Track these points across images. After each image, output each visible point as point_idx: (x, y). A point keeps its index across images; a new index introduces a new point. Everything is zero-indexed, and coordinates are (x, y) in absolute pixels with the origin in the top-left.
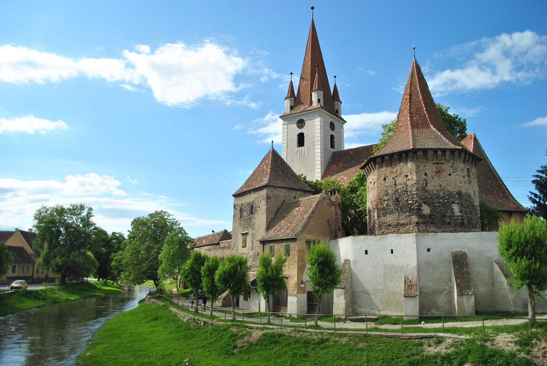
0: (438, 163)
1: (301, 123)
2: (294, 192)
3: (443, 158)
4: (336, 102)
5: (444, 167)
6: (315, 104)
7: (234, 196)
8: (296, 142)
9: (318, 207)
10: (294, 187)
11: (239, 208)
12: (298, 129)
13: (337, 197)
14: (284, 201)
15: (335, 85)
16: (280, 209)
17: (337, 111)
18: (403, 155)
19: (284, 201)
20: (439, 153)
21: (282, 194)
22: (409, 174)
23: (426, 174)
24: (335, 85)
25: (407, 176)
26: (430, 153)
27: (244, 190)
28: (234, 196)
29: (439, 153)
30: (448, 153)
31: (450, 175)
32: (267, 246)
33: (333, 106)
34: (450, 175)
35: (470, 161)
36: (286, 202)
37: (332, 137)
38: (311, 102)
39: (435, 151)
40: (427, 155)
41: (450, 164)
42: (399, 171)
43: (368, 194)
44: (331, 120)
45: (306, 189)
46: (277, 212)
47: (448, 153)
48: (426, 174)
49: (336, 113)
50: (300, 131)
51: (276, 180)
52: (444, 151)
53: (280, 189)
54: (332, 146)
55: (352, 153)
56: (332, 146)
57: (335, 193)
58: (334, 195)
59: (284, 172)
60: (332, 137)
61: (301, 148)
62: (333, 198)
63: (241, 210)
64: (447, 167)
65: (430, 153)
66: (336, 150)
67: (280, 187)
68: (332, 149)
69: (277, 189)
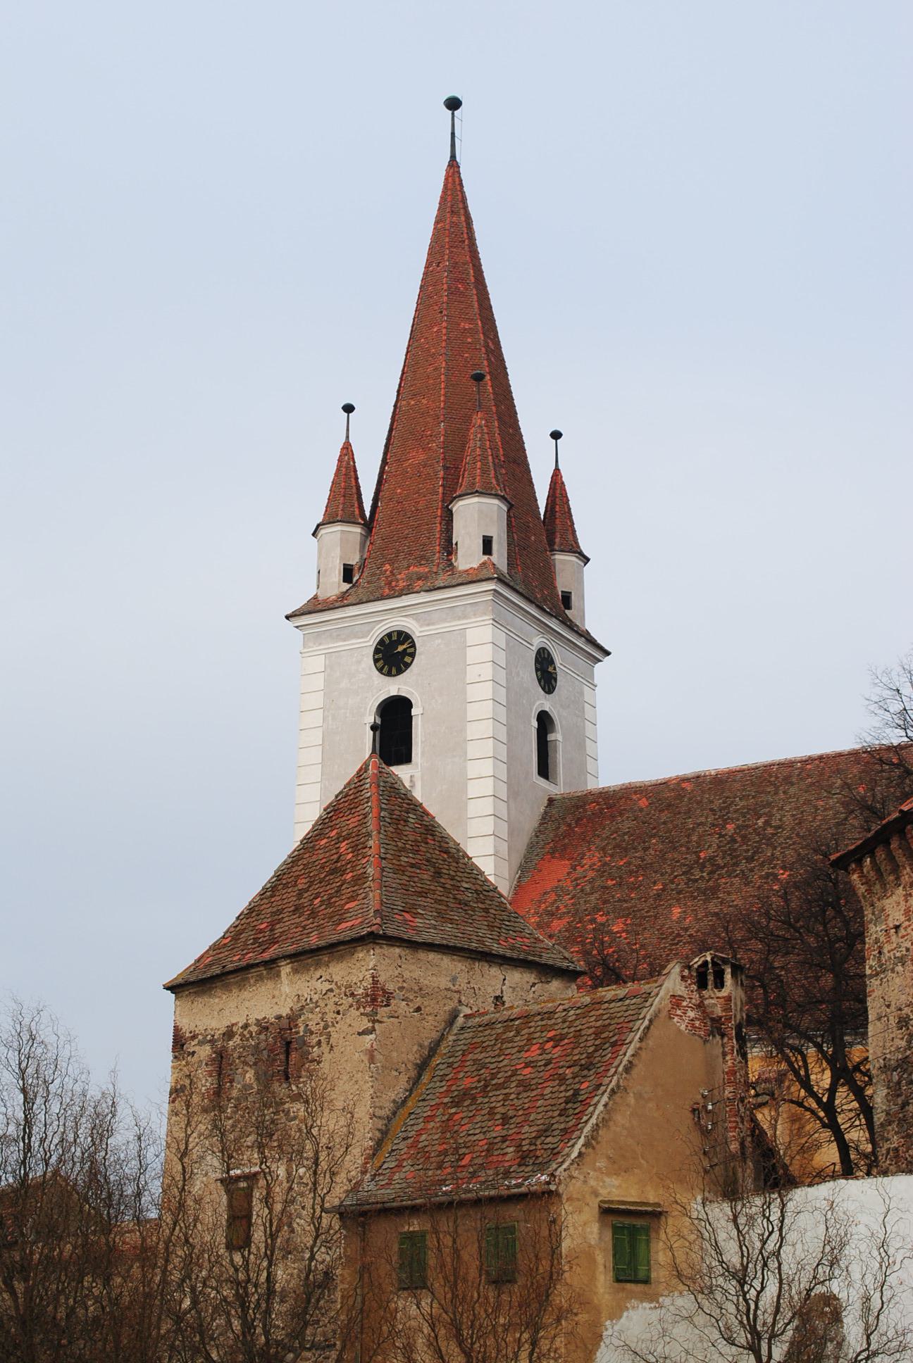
1: (394, 653)
2: (495, 971)
4: (560, 558)
6: (468, 556)
7: (174, 988)
9: (650, 1042)
10: (495, 948)
11: (205, 1052)
13: (728, 999)
14: (454, 1015)
15: (557, 473)
16: (433, 1050)
17: (566, 600)
19: (454, 1015)
21: (444, 982)
24: (557, 473)
27: (234, 961)
28: (174, 988)
32: (386, 1235)
33: (547, 574)
36: (460, 1020)
37: (545, 721)
38: (449, 548)
43: (873, 984)
44: (538, 641)
45: (546, 958)
46: (422, 1067)
49: (558, 606)
51: (410, 909)
53: (432, 956)
54: (544, 769)
55: (643, 803)
56: (544, 769)
58: (720, 984)
59: (438, 873)
60: (545, 721)
62: (714, 999)
63: (221, 1061)
66: (559, 788)
67: (431, 947)
68: (542, 782)
69: (422, 955)
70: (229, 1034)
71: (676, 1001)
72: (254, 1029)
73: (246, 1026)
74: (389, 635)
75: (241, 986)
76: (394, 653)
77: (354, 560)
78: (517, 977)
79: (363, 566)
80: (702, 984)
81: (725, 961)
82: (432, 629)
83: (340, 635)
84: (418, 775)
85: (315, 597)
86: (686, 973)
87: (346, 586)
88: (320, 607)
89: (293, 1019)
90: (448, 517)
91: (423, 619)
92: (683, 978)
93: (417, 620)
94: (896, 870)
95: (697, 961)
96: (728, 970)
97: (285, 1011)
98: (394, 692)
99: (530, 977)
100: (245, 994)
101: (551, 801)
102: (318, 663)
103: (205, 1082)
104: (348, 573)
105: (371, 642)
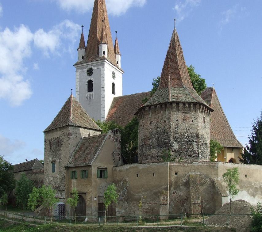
0: (185, 113)
1: (90, 72)
3: (189, 109)
5: (189, 115)
8: (86, 87)
9: (106, 143)
12: (87, 77)
13: (118, 136)
18: (163, 106)
20: (187, 105)
22: (166, 120)
23: (177, 121)
25: (165, 121)
26: (181, 105)
29: (187, 105)
30: (192, 105)
31: (192, 121)
34: (192, 121)
35: (206, 112)
38: (98, 54)
39: (184, 103)
40: (178, 107)
41: (193, 114)
42: (160, 118)
47: (192, 105)
48: (177, 121)
50: (90, 78)
52: (189, 104)
57: (117, 132)
58: (117, 134)
62: (116, 136)
64: (191, 115)
65: (181, 105)
70: (51, 140)
71: (110, 136)
72: (54, 139)
73: (53, 139)
75: (53, 132)
76: (90, 72)
77: (84, 55)
78: (91, 131)
80: (115, 134)
81: (118, 130)
82: (95, 68)
83: (81, 69)
85: (78, 62)
86: (112, 132)
87: (82, 60)
89: (59, 138)
91: (94, 66)
92: (111, 133)
93: (93, 66)
94: (141, 116)
95: (114, 130)
96: (118, 131)
97: (58, 136)
98: (90, 79)
99: (94, 131)
100: (53, 133)
101: (114, 98)
103: (49, 147)
104: (83, 57)
105: (86, 70)
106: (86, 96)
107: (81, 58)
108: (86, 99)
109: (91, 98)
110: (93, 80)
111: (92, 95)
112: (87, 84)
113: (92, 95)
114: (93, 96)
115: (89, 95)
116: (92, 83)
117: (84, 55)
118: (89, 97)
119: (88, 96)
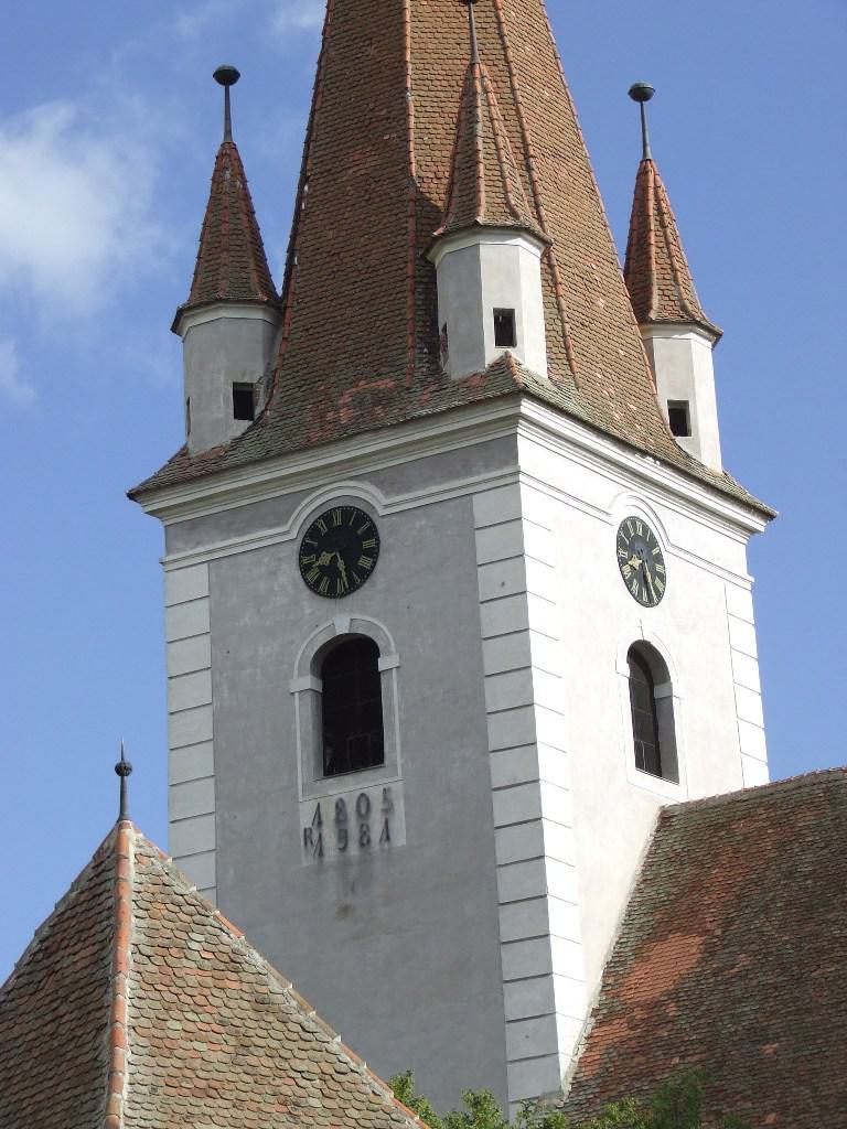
1: (340, 550)
12: (310, 604)
44: (622, 501)
50: (341, 620)
60: (646, 665)
61: (348, 787)
74: (327, 517)
76: (340, 550)
77: (254, 372)
79: (271, 381)
82: (403, 500)
84: (397, 788)
85: (184, 452)
88: (193, 471)
90: (427, 279)
91: (389, 481)
98: (342, 626)
102: (197, 580)
104: (243, 400)
105: (293, 529)
106: (306, 820)
107: (224, 406)
108: (308, 861)
109: (365, 842)
110: (384, 636)
111: (377, 806)
112: (307, 682)
113: (377, 806)
114: (388, 809)
115: (340, 807)
116: (375, 676)
117: (254, 372)
118: (343, 836)
119: (329, 815)
